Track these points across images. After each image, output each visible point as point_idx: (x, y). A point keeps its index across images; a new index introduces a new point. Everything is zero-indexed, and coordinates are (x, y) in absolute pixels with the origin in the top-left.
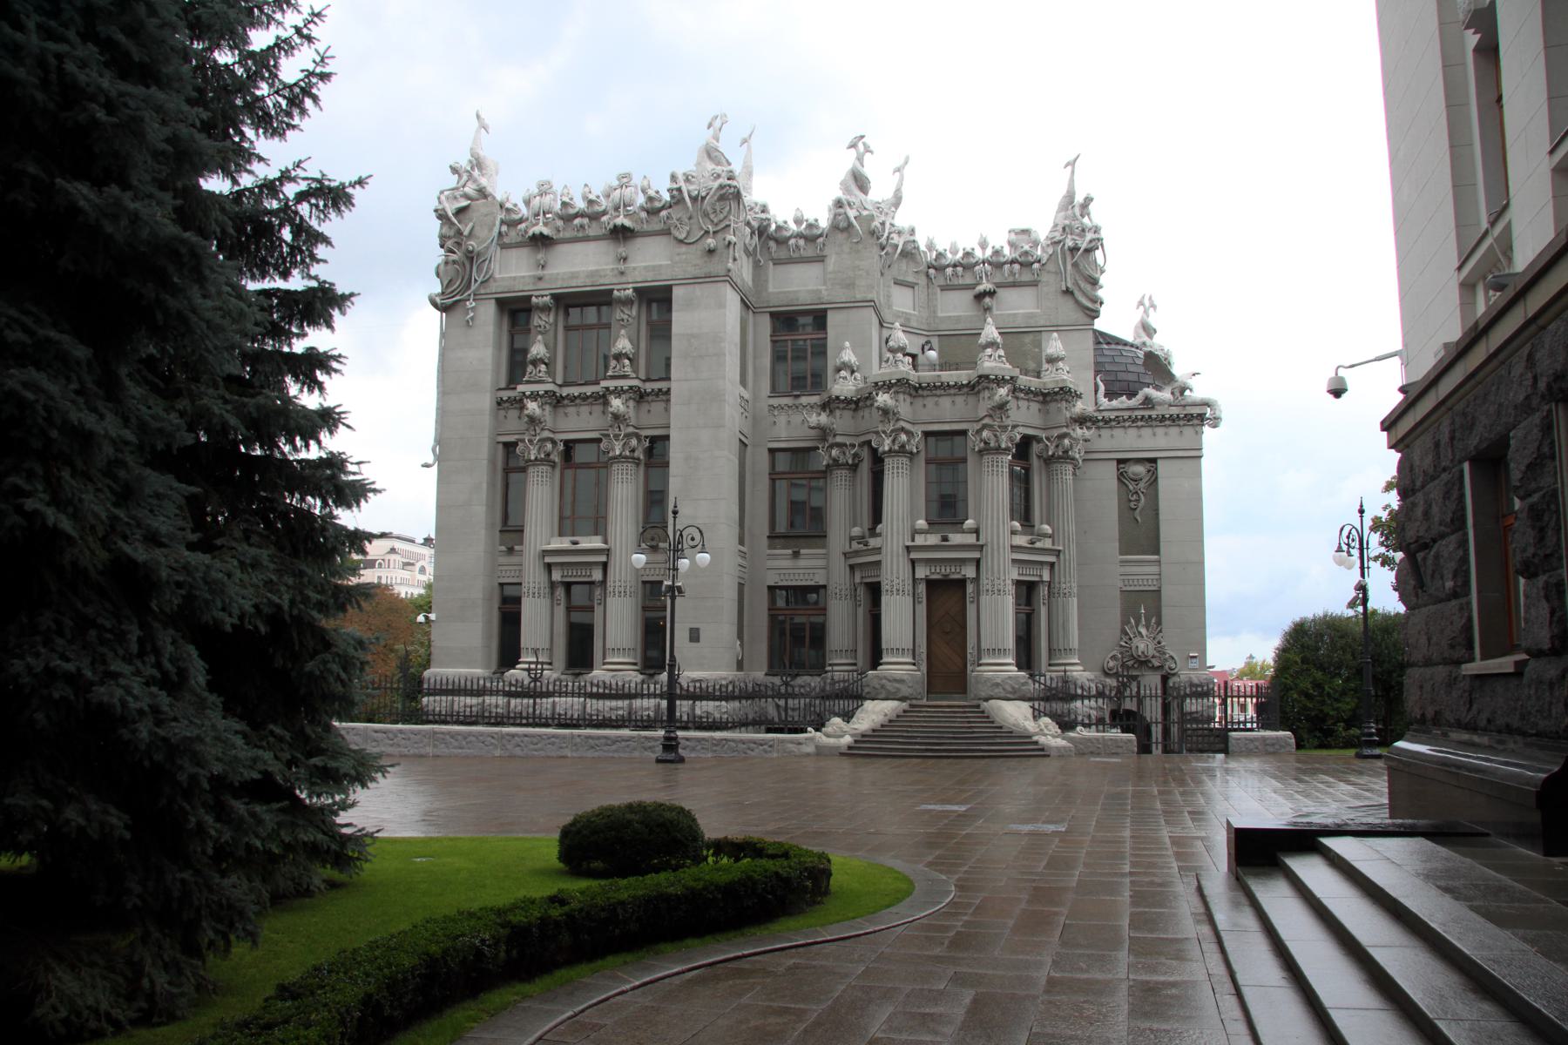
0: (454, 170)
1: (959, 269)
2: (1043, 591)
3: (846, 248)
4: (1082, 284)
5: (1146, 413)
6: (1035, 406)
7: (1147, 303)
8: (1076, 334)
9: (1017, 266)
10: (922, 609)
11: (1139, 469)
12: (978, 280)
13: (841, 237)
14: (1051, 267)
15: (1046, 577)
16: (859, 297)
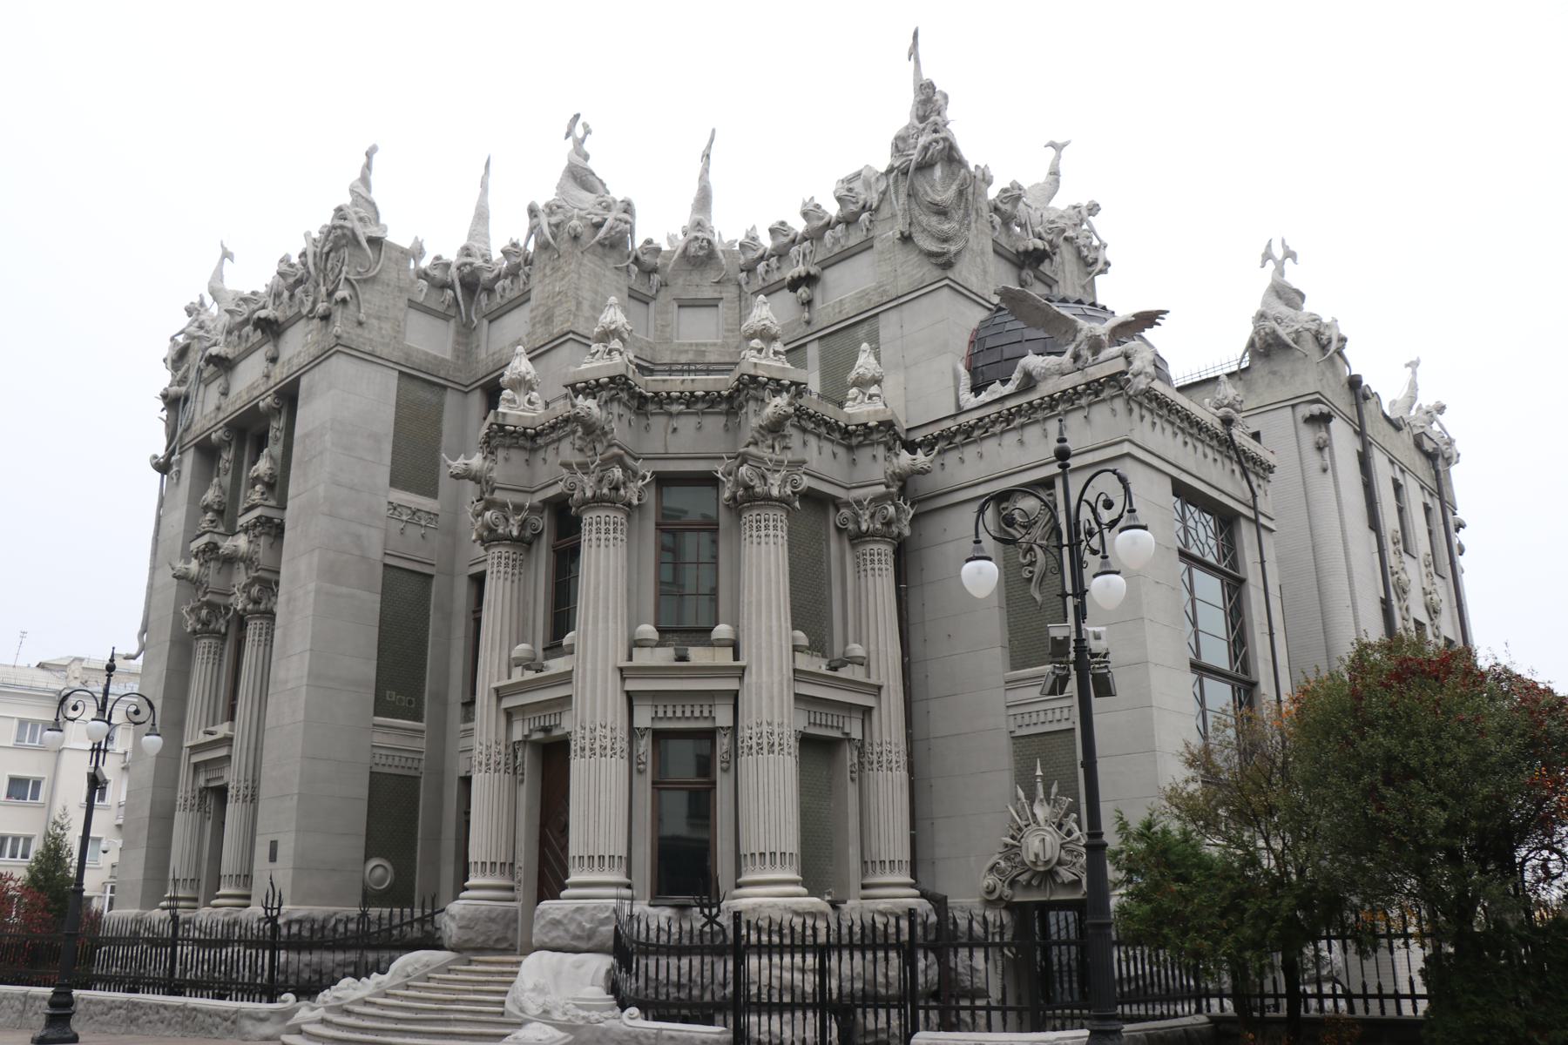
0: (189, 311)
1: (774, 260)
2: (723, 743)
3: (548, 271)
4: (924, 219)
5: (1023, 400)
6: (714, 424)
7: (1278, 253)
8: (924, 300)
9: (840, 227)
10: (527, 796)
11: (1029, 504)
12: (797, 263)
13: (545, 256)
14: (885, 212)
15: (723, 717)
16: (556, 331)
